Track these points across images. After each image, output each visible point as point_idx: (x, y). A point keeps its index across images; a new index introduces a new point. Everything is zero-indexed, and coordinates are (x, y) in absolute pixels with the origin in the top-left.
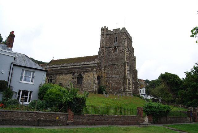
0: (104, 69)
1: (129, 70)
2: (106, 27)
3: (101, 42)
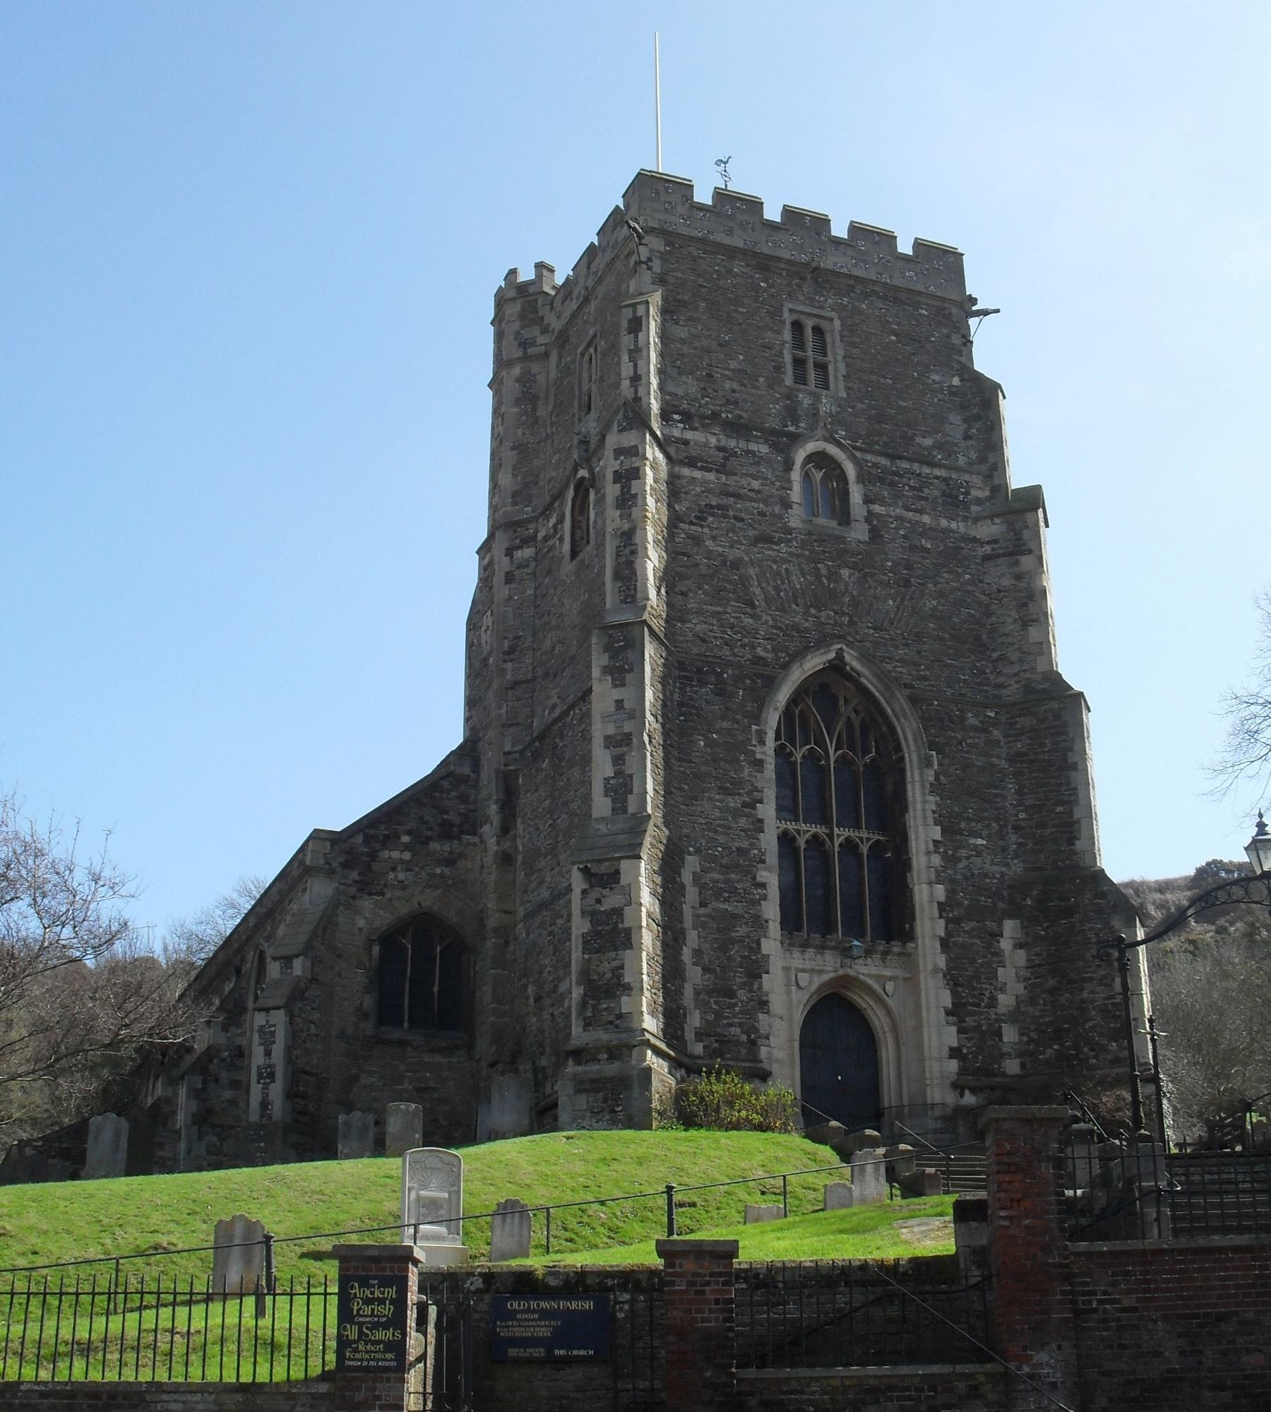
0: (493, 809)
2: (526, 274)
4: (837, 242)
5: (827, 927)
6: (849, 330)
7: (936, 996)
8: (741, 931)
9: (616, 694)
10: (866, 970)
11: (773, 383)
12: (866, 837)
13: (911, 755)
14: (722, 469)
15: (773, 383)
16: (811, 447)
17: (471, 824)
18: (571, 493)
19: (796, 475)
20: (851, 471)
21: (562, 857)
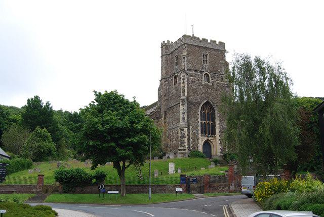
1: (186, 112)
2: (166, 42)
3: (162, 69)
5: (205, 133)
7: (218, 142)
12: (211, 122)
13: (216, 113)
14: (194, 77)
17: (160, 117)
19: (203, 77)
20: (210, 76)
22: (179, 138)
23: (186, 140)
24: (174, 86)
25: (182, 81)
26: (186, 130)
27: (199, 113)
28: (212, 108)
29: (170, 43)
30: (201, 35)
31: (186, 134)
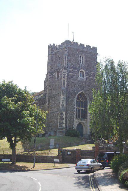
0: (47, 102)
2: (52, 45)
3: (48, 66)
4: (85, 47)
5: (79, 117)
6: (85, 57)
8: (72, 118)
9: (63, 96)
10: (83, 121)
11: (78, 63)
12: (83, 109)
13: (88, 101)
15: (78, 63)
16: (81, 70)
17: (45, 103)
18: (57, 72)
20: (85, 72)
21: (55, 109)
22: (59, 120)
23: (64, 121)
24: (56, 80)
25: (63, 76)
26: (64, 113)
27: (75, 101)
28: (85, 98)
29: (55, 46)
30: (79, 41)
31: (64, 117)
